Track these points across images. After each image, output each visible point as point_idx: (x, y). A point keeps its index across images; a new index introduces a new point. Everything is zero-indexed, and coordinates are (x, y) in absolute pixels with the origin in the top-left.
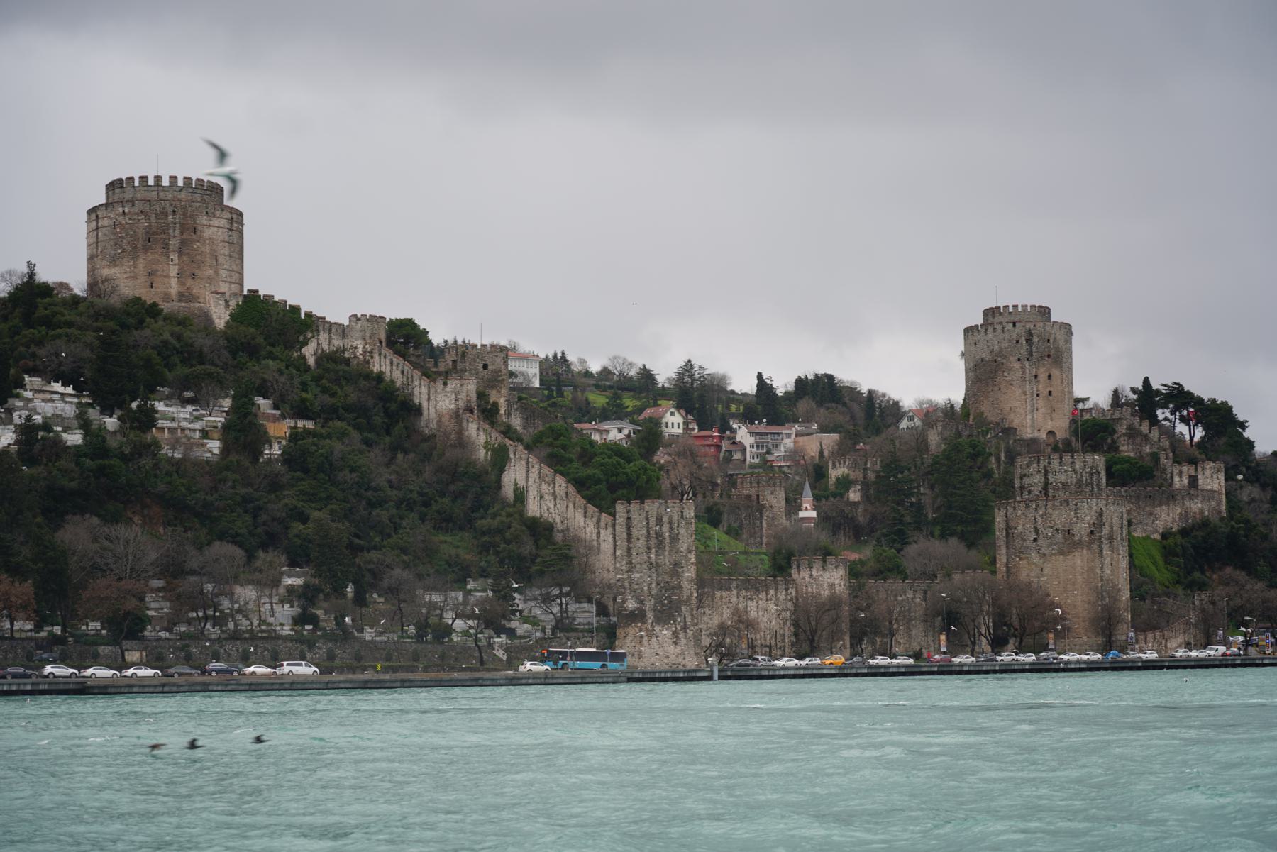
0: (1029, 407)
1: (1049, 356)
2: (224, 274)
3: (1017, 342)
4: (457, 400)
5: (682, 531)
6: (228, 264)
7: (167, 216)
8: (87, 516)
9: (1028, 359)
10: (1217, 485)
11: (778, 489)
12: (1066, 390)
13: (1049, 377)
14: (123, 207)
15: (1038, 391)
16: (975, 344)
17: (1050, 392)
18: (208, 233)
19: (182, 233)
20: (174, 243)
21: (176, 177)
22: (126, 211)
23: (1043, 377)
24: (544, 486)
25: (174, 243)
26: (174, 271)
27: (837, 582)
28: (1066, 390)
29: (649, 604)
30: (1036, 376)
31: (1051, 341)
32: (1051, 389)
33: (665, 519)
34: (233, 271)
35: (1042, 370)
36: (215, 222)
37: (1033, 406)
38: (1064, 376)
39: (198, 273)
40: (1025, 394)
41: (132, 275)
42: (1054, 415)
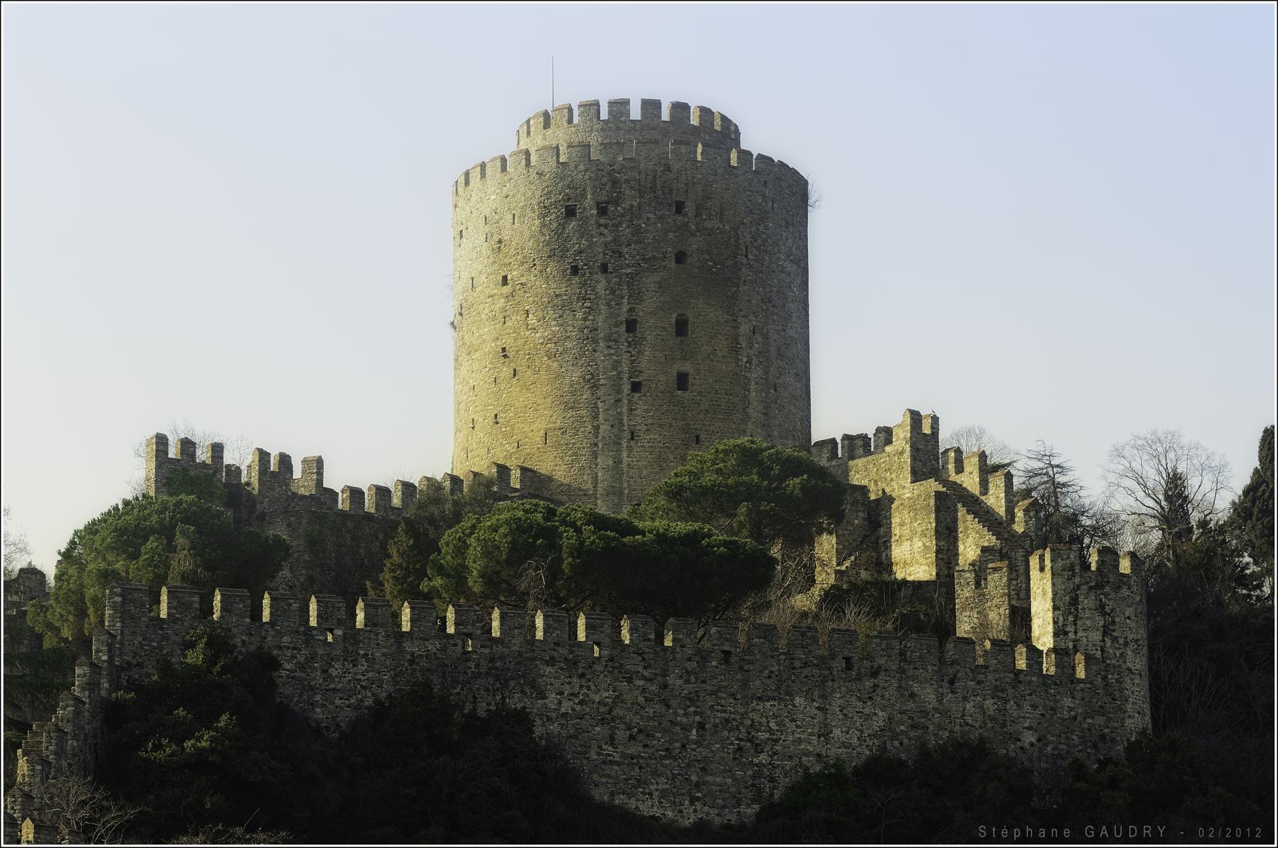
0: (604, 428)
1: (680, 257)
3: (570, 212)
9: (604, 268)
10: (1096, 636)
12: (756, 373)
13: (681, 327)
17: (682, 381)
23: (654, 328)
28: (756, 373)
30: (631, 326)
31: (690, 208)
32: (688, 367)
35: (650, 301)
37: (617, 423)
38: (745, 329)
40: (595, 387)
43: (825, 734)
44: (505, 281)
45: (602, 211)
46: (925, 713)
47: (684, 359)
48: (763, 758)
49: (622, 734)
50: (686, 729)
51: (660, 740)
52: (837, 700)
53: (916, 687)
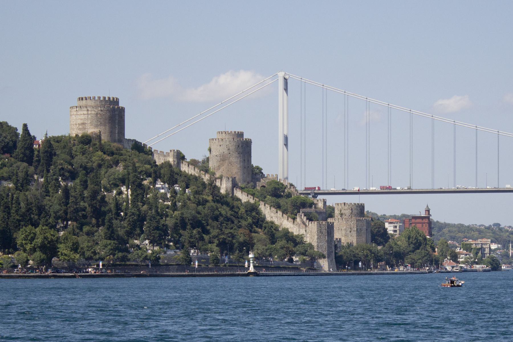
3: (239, 146)
4: (232, 184)
5: (332, 231)
7: (115, 112)
14: (101, 108)
16: (220, 146)
17: (248, 166)
19: (119, 118)
20: (117, 121)
22: (102, 109)
24: (272, 215)
25: (117, 121)
26: (117, 132)
29: (325, 253)
33: (329, 227)
41: (104, 132)
44: (230, 153)
45: (242, 146)
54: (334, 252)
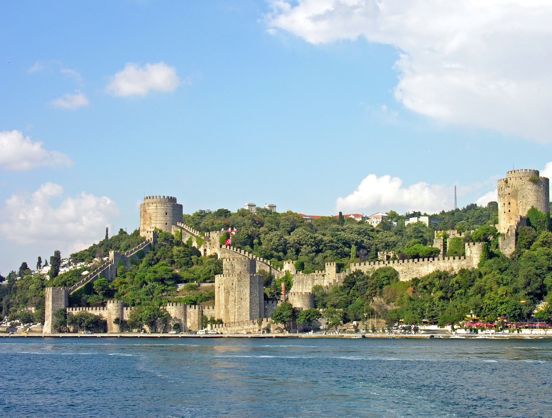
2: (153, 222)
6: (155, 219)
8: (411, 279)
11: (332, 268)
13: (509, 203)
15: (504, 210)
17: (509, 210)
18: (148, 211)
21: (160, 196)
23: (507, 204)
27: (110, 308)
31: (510, 187)
32: (510, 209)
34: (157, 220)
35: (506, 200)
36: (150, 208)
38: (519, 202)
39: (146, 223)
42: (511, 221)
43: (428, 270)
46: (441, 266)
47: (510, 208)
48: (420, 273)
49: (403, 273)
50: (411, 271)
51: (408, 273)
52: (429, 267)
53: (440, 263)
54: (51, 315)
